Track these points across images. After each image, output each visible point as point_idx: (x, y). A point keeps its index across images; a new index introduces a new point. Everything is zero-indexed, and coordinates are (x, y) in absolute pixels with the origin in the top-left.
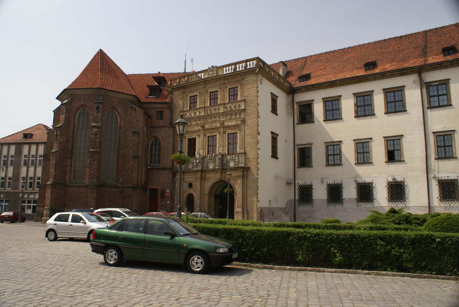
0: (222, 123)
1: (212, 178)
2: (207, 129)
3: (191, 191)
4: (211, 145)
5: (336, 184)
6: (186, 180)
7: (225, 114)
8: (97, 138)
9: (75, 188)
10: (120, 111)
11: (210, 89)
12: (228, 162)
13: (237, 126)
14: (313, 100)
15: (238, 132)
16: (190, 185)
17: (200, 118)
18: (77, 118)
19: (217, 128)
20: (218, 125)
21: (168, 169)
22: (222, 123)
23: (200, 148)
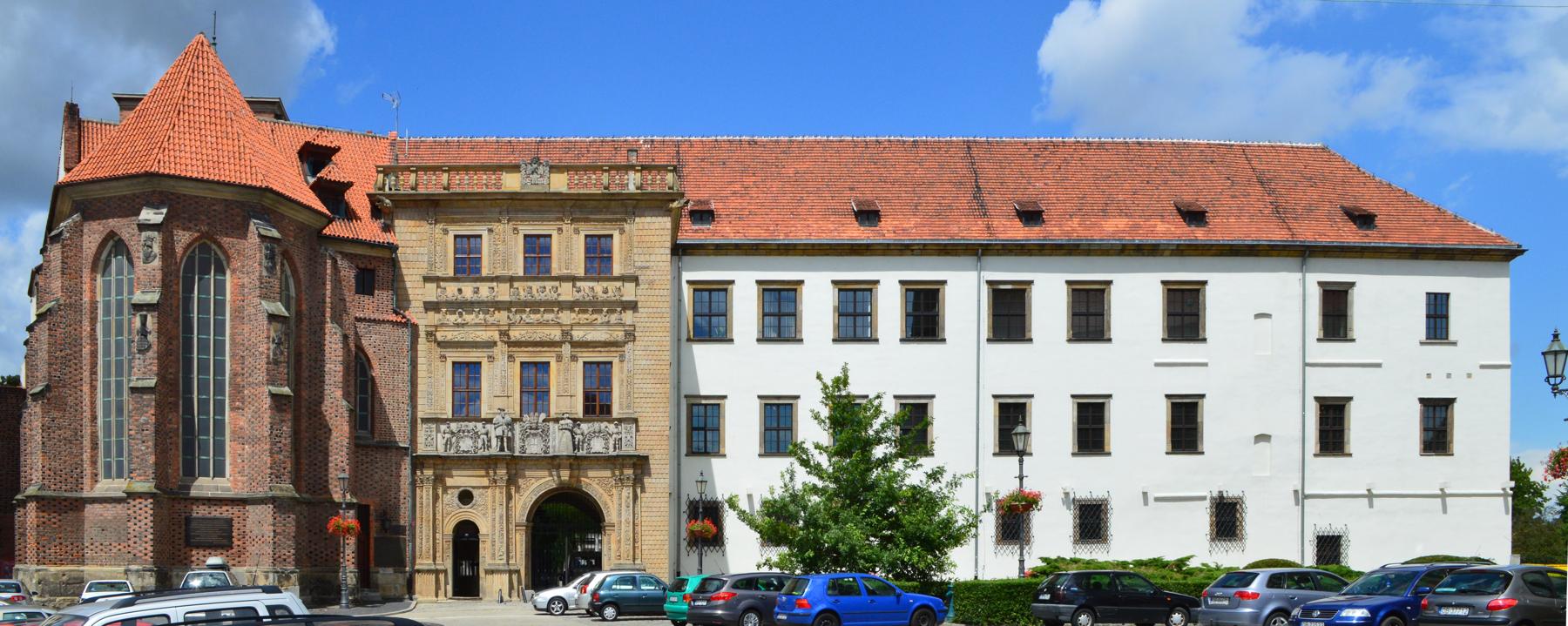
1: (538, 478)
2: (518, 344)
4: (535, 387)
12: (587, 438)
15: (616, 361)
17: (498, 306)
20: (555, 334)
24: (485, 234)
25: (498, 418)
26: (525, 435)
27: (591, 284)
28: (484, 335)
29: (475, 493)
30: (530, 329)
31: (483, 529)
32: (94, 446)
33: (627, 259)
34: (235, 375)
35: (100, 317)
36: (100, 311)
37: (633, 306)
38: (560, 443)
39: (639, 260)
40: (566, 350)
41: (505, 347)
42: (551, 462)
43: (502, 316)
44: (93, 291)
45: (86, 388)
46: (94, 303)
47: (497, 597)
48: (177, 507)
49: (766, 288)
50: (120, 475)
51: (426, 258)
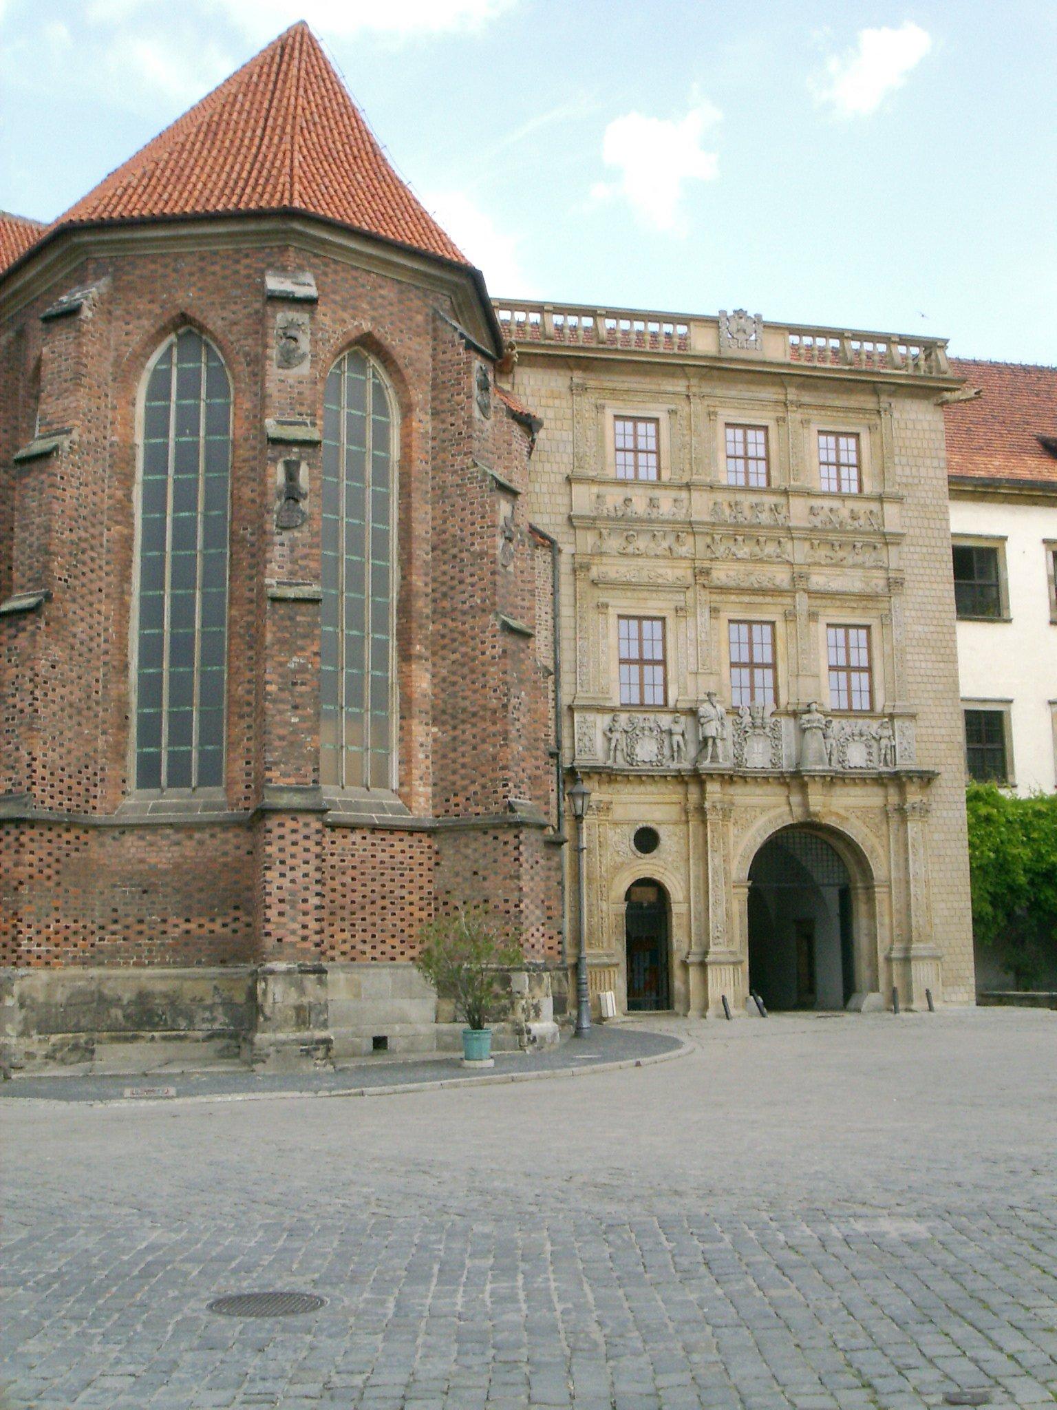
0: (799, 578)
1: (764, 809)
2: (723, 590)
3: (647, 866)
6: (618, 812)
9: (356, 837)
11: (732, 412)
13: (867, 598)
16: (646, 840)
19: (777, 592)
20: (781, 577)
22: (799, 578)
24: (663, 417)
26: (743, 735)
29: (663, 832)
40: (802, 602)
41: (704, 596)
50: (179, 778)
51: (569, 449)
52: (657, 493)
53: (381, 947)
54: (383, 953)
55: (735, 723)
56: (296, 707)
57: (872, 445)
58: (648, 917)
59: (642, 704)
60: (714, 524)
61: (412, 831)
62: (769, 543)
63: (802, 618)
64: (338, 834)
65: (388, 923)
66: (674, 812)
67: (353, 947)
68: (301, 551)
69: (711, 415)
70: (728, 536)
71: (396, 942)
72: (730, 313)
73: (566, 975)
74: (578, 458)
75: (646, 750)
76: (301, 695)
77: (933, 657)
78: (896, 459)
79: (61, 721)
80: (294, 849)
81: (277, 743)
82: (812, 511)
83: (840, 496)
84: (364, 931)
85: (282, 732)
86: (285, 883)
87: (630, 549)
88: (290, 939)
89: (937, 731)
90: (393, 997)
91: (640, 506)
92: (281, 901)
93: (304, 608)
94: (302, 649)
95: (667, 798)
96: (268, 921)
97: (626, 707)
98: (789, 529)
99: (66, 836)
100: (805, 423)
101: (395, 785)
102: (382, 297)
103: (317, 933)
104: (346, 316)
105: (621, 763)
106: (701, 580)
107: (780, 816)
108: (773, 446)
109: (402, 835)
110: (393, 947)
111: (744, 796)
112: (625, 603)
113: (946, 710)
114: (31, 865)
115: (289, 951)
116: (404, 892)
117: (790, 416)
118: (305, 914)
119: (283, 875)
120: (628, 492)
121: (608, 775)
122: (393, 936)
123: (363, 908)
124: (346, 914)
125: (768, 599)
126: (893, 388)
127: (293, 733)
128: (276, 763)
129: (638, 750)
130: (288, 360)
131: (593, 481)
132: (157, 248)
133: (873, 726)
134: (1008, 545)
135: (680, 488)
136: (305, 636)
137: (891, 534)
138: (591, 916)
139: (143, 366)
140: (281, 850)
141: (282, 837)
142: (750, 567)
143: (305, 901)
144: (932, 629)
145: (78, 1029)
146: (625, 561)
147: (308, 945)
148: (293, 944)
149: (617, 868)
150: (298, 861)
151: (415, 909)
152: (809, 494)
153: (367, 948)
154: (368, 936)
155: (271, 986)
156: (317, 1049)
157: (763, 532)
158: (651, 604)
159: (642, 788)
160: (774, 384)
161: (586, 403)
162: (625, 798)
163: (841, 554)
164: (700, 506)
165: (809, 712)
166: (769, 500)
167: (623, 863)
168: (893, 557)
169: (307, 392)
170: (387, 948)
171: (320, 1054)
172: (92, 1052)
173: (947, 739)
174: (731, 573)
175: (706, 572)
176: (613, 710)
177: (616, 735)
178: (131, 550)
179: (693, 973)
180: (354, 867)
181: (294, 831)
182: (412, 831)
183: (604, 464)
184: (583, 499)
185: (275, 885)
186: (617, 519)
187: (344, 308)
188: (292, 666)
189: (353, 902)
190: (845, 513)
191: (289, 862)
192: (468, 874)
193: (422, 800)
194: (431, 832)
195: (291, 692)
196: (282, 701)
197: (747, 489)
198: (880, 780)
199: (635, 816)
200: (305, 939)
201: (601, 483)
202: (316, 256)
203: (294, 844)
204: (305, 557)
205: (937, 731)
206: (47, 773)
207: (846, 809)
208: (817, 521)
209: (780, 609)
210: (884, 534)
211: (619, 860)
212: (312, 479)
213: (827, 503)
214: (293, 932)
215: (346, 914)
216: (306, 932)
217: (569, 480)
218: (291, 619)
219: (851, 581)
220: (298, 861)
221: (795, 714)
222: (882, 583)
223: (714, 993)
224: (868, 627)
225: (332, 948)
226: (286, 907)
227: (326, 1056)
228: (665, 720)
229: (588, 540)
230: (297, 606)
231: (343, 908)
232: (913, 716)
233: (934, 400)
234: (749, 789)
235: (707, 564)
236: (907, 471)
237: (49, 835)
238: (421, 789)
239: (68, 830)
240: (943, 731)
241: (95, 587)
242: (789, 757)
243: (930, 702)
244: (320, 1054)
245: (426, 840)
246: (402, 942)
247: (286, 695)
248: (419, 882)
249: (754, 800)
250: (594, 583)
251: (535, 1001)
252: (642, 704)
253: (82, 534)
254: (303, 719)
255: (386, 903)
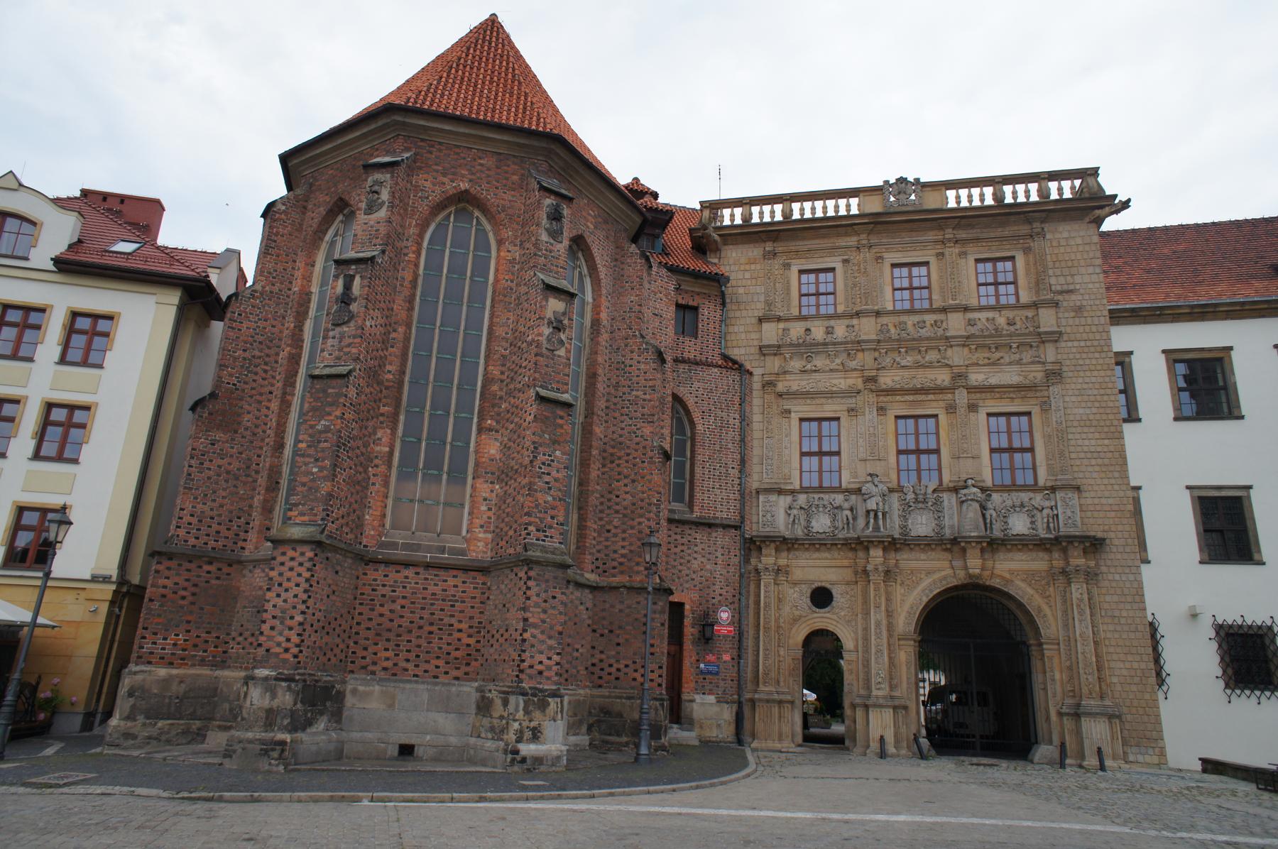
0: (959, 377)
1: (929, 573)
5: (1250, 627)
6: (798, 574)
7: (966, 341)
8: (561, 342)
9: (410, 572)
10: (598, 260)
14: (1131, 353)
18: (425, 244)
19: (939, 390)
20: (943, 377)
21: (725, 527)
22: (959, 377)
23: (862, 456)
25: (867, 488)
26: (907, 508)
27: (990, 315)
28: (842, 383)
29: (836, 591)
30: (906, 373)
31: (848, 641)
32: (273, 486)
33: (1039, 282)
34: (487, 381)
35: (312, 313)
36: (313, 306)
37: (1055, 337)
38: (961, 518)
39: (1056, 282)
40: (962, 397)
41: (872, 398)
42: (954, 544)
43: (866, 359)
44: (308, 278)
45: (275, 405)
46: (306, 297)
47: (874, 746)
48: (372, 575)
49: (1173, 357)
51: (762, 298)
52: (832, 323)
53: (424, 666)
54: (426, 671)
55: (900, 499)
56: (317, 460)
57: (1027, 264)
58: (822, 662)
59: (821, 487)
60: (879, 341)
61: (466, 569)
62: (930, 352)
63: (962, 411)
64: (391, 568)
65: (435, 646)
66: (848, 574)
67: (395, 665)
68: (347, 341)
69: (879, 259)
70: (893, 350)
71: (441, 663)
72: (892, 181)
73: (662, 705)
74: (769, 304)
75: (821, 523)
76: (323, 450)
77: (1097, 435)
78: (1051, 272)
79: (217, 483)
80: (289, 574)
81: (299, 489)
82: (971, 323)
83: (998, 308)
84: (408, 651)
85: (305, 480)
86: (280, 602)
87: (809, 367)
88: (277, 650)
89: (1104, 501)
90: (428, 710)
91: (818, 333)
92: (274, 617)
93: (334, 382)
94: (329, 414)
95: (838, 563)
96: (262, 633)
97: (804, 490)
98: (947, 338)
99: (206, 568)
100: (963, 254)
101: (464, 533)
102: (481, 165)
103: (297, 646)
104: (445, 180)
105: (799, 532)
106: (870, 386)
107: (945, 578)
108: (934, 276)
109: (455, 572)
110: (437, 667)
111: (909, 561)
112: (805, 408)
113: (1113, 481)
114: (165, 587)
115: (273, 660)
116: (453, 621)
117: (947, 251)
118: (291, 629)
119: (278, 596)
120: (808, 324)
121: (786, 544)
122: (438, 658)
123: (410, 631)
124: (392, 636)
125: (931, 397)
126: (1044, 215)
127: (313, 480)
128: (296, 505)
129: (814, 523)
130: (370, 209)
131: (779, 319)
132: (333, 158)
133: (1038, 499)
134: (1233, 353)
135: (852, 317)
136: (331, 405)
137: (1046, 333)
138: (766, 658)
139: (322, 240)
140: (281, 574)
141: (282, 564)
142: (913, 372)
143: (292, 618)
144: (1094, 410)
145: (193, 717)
146: (805, 376)
147: (288, 656)
148: (277, 655)
149: (795, 620)
150: (292, 584)
151: (463, 635)
152: (966, 309)
153: (410, 666)
154: (412, 656)
155: (252, 689)
156: (273, 750)
157: (925, 344)
158: (827, 408)
159: (817, 555)
160: (932, 229)
161: (777, 263)
162: (802, 562)
163: (998, 355)
164: (868, 328)
165: (966, 487)
166: (930, 318)
167: (801, 617)
168: (1050, 353)
169: (382, 229)
170: (431, 667)
171: (275, 754)
172: (205, 736)
173: (1116, 508)
174: (896, 379)
175: (873, 380)
176: (793, 492)
177: (795, 512)
178: (298, 364)
179: (860, 713)
180: (404, 597)
181: (292, 559)
182: (466, 569)
183: (789, 306)
184: (771, 333)
185: (271, 603)
186: (799, 345)
187: (445, 175)
188: (319, 427)
189: (400, 626)
190: (1001, 321)
191: (285, 584)
192: (500, 606)
193: (481, 544)
194: (483, 569)
195: (316, 447)
196: (309, 456)
197: (912, 311)
198: (1042, 545)
199: (811, 577)
200: (287, 650)
201: (787, 320)
202: (422, 140)
203: (291, 569)
204: (349, 345)
205: (1104, 501)
206: (194, 520)
207: (1011, 572)
208: (973, 330)
209: (942, 404)
210: (1039, 334)
211: (797, 613)
212: (362, 287)
213: (983, 315)
214: (279, 644)
215: (392, 636)
216: (289, 645)
217: (760, 320)
218: (325, 391)
219: (1009, 376)
220: (292, 584)
221: (955, 490)
222: (1040, 375)
223: (875, 733)
224: (1028, 414)
225: (375, 663)
226: (277, 622)
227: (280, 757)
228: (839, 499)
229: (774, 364)
230: (329, 381)
231: (389, 630)
232: (1078, 488)
233: (1087, 220)
234: (916, 554)
235: (873, 373)
236: (1062, 280)
237: (186, 565)
238: (481, 535)
239: (210, 563)
240: (1111, 501)
241: (267, 389)
242: (952, 527)
243: (1095, 475)
244: (275, 754)
245: (480, 579)
246: (447, 663)
247: (311, 451)
248: (469, 612)
249: (914, 564)
250: (780, 395)
251: (533, 724)
252: (821, 487)
253: (257, 353)
254: (322, 469)
255: (434, 628)
